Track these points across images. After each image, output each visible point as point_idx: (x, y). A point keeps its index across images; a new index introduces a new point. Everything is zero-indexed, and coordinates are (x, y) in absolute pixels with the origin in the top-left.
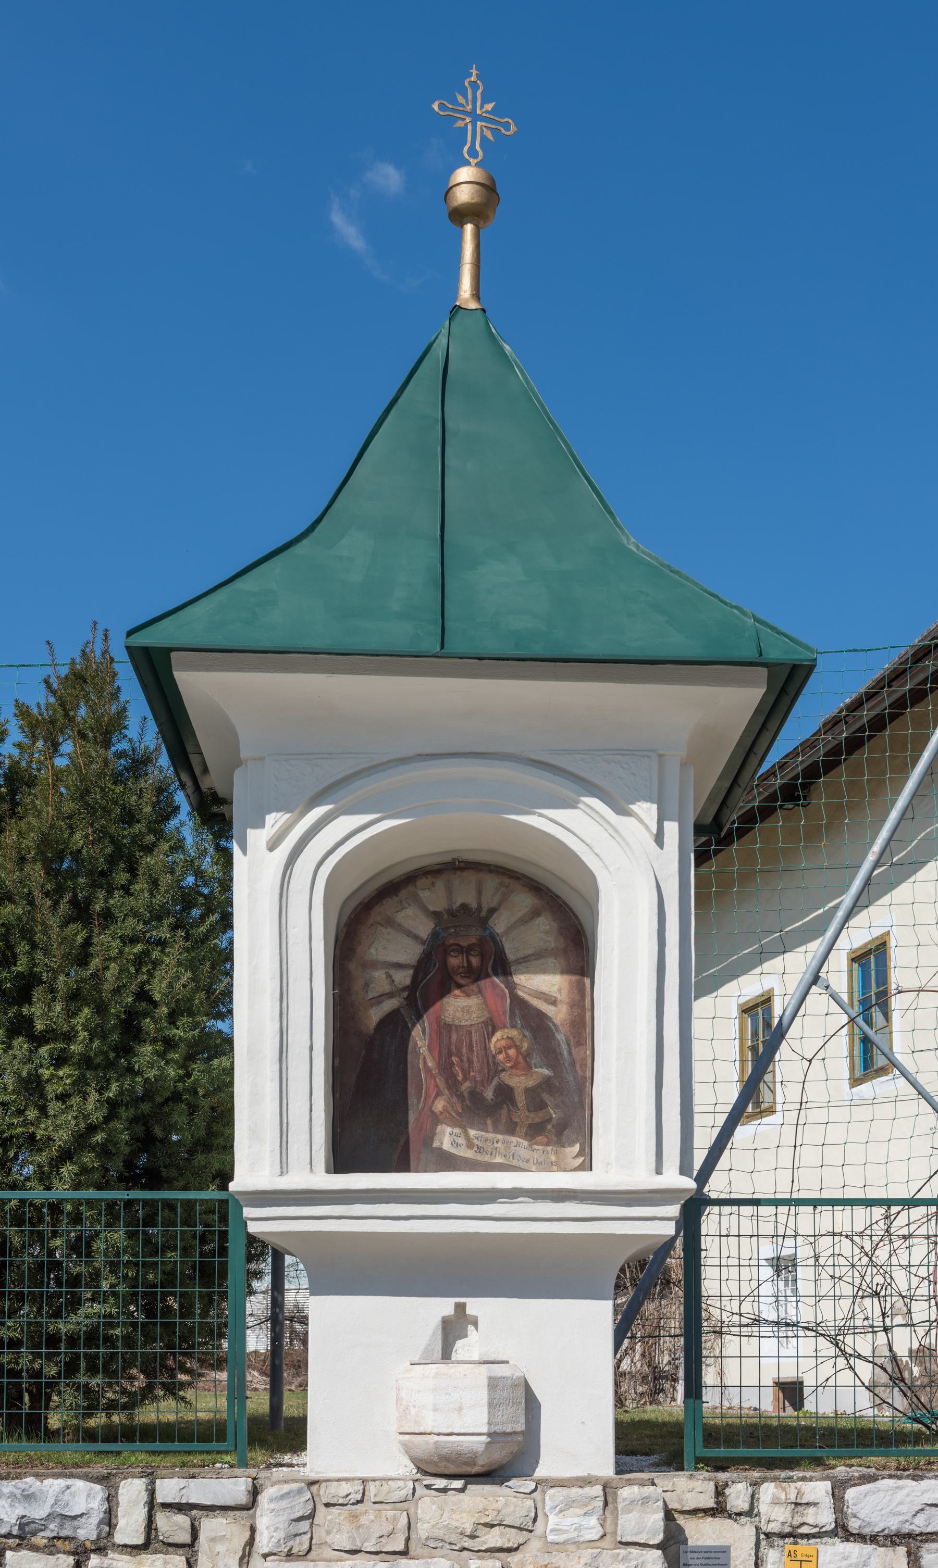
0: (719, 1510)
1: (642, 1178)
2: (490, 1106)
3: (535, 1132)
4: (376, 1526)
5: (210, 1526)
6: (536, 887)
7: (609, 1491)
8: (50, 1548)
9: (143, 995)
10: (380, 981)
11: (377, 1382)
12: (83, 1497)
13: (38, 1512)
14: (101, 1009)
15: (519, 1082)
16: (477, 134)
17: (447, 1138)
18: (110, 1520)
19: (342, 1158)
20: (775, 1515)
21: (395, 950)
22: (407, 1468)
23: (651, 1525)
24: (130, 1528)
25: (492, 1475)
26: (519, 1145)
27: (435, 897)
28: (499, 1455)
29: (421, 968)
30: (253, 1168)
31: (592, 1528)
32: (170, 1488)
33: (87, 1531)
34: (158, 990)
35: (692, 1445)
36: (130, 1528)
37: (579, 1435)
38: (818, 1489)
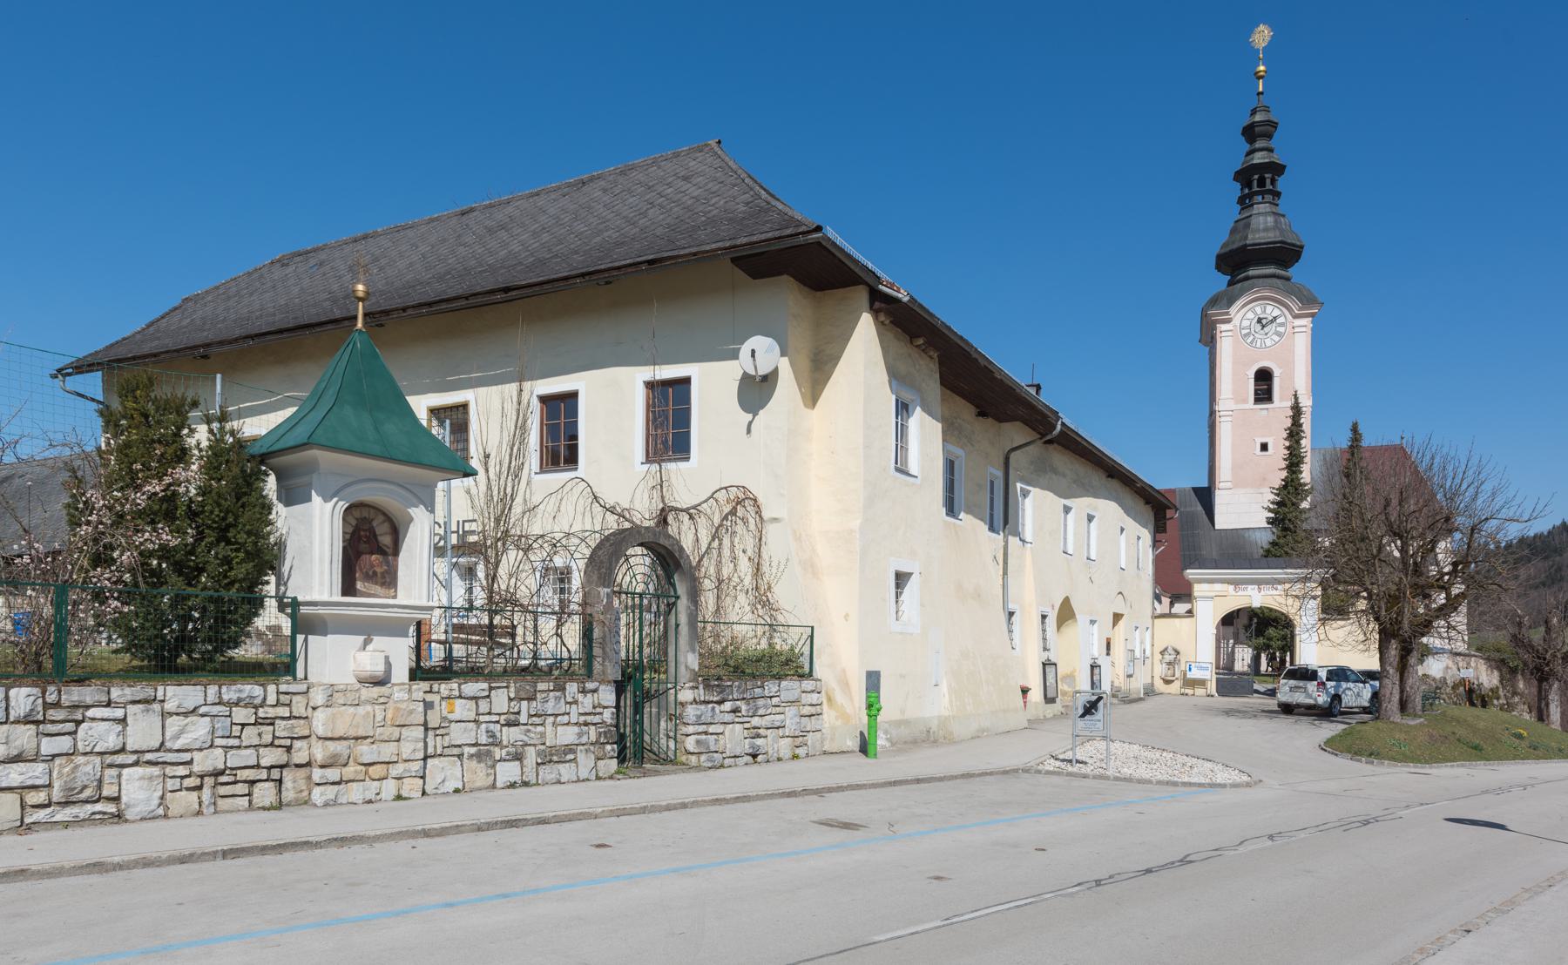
2: (371, 577)
3: (383, 585)
8: (246, 706)
11: (333, 661)
12: (258, 691)
13: (244, 695)
15: (379, 570)
17: (359, 585)
18: (265, 699)
20: (445, 693)
22: (354, 681)
24: (272, 699)
26: (378, 589)
32: (283, 688)
36: (272, 699)
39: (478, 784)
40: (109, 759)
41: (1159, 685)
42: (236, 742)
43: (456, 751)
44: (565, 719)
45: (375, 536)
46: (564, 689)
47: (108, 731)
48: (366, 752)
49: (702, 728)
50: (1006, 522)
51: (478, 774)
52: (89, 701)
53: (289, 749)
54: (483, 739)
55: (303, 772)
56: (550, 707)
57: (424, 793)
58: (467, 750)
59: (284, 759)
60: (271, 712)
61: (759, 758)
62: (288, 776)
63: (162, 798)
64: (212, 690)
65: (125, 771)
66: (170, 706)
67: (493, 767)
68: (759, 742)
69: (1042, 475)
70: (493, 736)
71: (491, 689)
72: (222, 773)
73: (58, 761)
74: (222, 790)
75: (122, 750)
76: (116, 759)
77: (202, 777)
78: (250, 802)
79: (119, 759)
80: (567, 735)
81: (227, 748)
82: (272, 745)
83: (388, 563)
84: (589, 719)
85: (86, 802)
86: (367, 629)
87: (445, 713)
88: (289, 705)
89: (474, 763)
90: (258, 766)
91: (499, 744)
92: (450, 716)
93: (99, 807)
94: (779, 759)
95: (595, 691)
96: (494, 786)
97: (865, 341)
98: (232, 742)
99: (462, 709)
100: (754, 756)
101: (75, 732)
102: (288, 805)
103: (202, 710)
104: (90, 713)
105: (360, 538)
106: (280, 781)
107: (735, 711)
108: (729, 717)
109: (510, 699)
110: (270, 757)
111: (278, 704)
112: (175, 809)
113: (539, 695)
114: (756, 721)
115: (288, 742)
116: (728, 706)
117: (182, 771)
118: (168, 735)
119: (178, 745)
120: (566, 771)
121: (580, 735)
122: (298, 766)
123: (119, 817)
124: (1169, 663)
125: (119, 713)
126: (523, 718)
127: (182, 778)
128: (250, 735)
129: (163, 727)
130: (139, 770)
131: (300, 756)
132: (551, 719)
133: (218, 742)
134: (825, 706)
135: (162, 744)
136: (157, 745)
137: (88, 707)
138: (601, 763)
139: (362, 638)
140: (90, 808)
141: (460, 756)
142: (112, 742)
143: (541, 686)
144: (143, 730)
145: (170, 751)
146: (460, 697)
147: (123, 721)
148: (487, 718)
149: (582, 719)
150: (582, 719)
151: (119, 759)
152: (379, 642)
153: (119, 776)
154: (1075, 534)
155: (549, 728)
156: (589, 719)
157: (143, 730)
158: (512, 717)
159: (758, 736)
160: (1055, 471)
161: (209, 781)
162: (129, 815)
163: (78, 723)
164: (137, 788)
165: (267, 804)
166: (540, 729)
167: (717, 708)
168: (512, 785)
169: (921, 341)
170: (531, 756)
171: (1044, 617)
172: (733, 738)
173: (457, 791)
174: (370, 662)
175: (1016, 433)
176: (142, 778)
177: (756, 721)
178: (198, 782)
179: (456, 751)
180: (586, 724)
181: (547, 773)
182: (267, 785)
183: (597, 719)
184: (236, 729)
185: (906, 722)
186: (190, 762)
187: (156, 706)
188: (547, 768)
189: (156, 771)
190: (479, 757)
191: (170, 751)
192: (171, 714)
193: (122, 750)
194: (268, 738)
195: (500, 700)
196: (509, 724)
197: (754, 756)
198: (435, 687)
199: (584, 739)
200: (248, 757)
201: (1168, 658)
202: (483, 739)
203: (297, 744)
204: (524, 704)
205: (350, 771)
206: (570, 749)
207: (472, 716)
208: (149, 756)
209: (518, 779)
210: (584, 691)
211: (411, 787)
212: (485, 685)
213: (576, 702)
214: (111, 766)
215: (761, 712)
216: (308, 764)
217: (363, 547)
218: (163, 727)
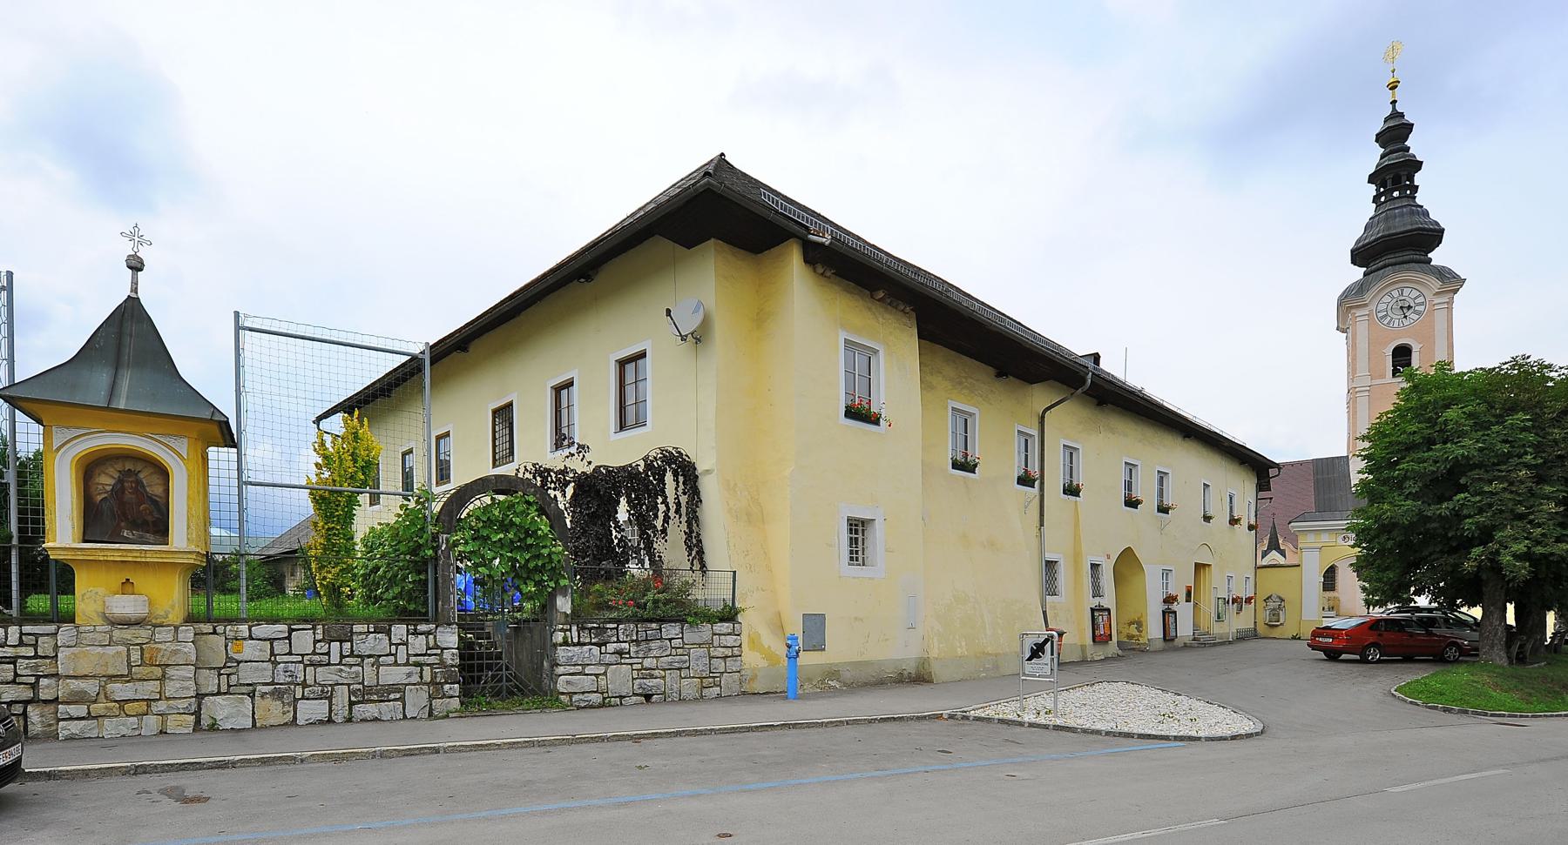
0: (215, 632)
3: (155, 533)
7: (176, 628)
20: (231, 634)
21: (106, 481)
26: (151, 537)
27: (119, 466)
39: (272, 722)
43: (245, 689)
48: (120, 690)
51: (274, 711)
55: (51, 708)
59: (29, 694)
68: (650, 683)
71: (291, 631)
80: (392, 675)
82: (14, 682)
86: (127, 577)
88: (35, 646)
89: (268, 700)
92: (236, 656)
99: (249, 650)
100: (648, 697)
107: (620, 653)
108: (614, 658)
109: (316, 642)
111: (21, 644)
114: (648, 663)
115: (32, 680)
116: (611, 647)
120: (388, 709)
122: (46, 702)
138: (436, 703)
141: (252, 695)
146: (251, 638)
148: (286, 658)
149: (412, 659)
159: (652, 677)
167: (596, 650)
180: (416, 664)
183: (432, 660)
197: (648, 697)
198: (220, 629)
201: (1272, 605)
202: (281, 678)
203: (44, 682)
205: (97, 708)
206: (395, 688)
210: (416, 633)
213: (406, 644)
215: (654, 653)
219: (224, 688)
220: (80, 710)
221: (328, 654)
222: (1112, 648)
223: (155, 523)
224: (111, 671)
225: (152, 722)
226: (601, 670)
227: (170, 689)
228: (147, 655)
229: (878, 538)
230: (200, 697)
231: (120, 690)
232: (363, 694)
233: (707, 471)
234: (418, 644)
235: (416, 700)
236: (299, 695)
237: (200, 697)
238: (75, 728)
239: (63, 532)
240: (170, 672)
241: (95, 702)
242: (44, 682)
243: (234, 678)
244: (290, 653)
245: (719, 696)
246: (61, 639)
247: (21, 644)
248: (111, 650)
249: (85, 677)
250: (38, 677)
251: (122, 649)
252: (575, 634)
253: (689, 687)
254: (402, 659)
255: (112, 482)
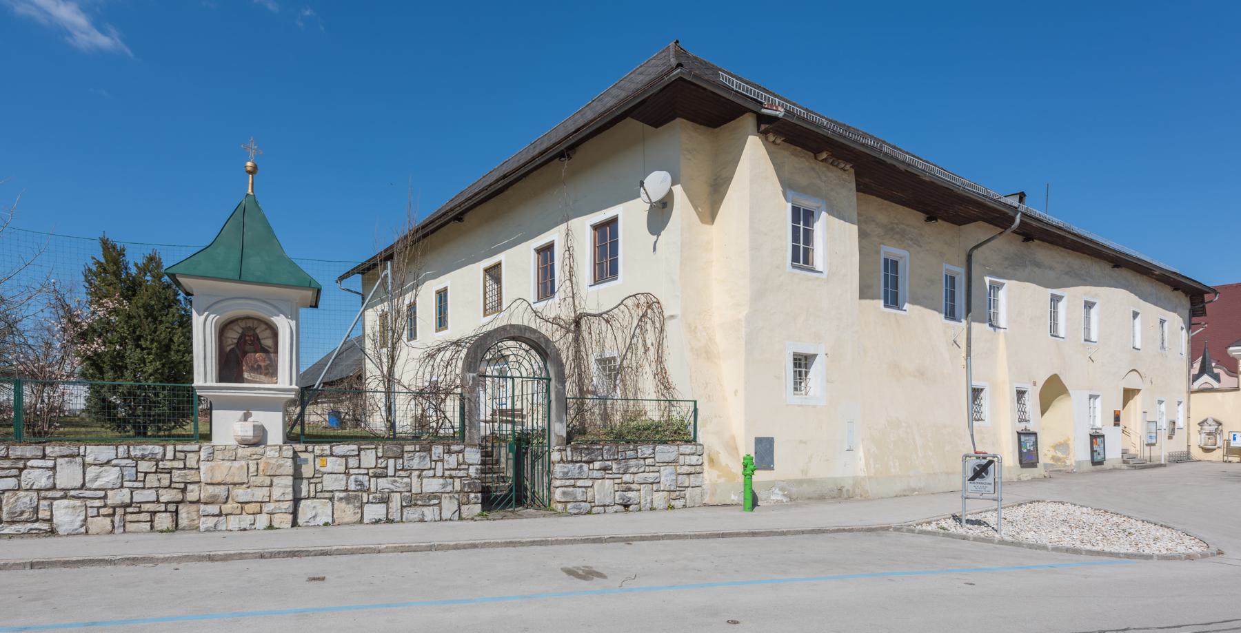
0: (306, 451)
1: (287, 386)
2: (256, 369)
3: (266, 374)
4: (227, 454)
5: (189, 455)
6: (266, 323)
8: (150, 460)
9: (171, 340)
10: (230, 341)
12: (158, 449)
14: (160, 343)
15: (262, 364)
16: (252, 153)
17: (246, 375)
18: (164, 455)
19: (221, 379)
20: (318, 452)
21: (233, 335)
23: (290, 453)
24: (170, 455)
25: (256, 445)
27: (243, 324)
28: (256, 440)
29: (239, 339)
30: (198, 381)
31: (277, 454)
32: (179, 447)
33: (159, 457)
34: (175, 339)
35: (303, 438)
36: (170, 455)
37: (276, 435)
38: (327, 447)
39: (346, 520)
40: (43, 494)
41: (1196, 453)
42: (141, 485)
43: (327, 495)
44: (431, 473)
45: (258, 339)
46: (430, 450)
47: (41, 476)
48: (241, 494)
49: (568, 482)
50: (969, 310)
51: (347, 512)
52: (28, 455)
53: (184, 490)
54: (352, 486)
55: (194, 507)
56: (415, 463)
57: (295, 524)
58: (337, 494)
59: (180, 497)
60: (168, 465)
61: (631, 508)
62: (183, 509)
63: (85, 520)
64: (122, 449)
65: (55, 503)
66: (89, 459)
67: (362, 507)
68: (630, 494)
69: (1016, 269)
70: (361, 484)
71: (360, 450)
72: (130, 505)
73: (6, 494)
74: (129, 517)
75: (54, 488)
76: (51, 492)
77: (114, 508)
78: (152, 527)
79: (50, 494)
81: (132, 490)
82: (169, 487)
83: (270, 359)
84: (453, 473)
85: (26, 521)
86: (247, 407)
87: (318, 467)
89: (343, 505)
90: (158, 501)
91: (368, 491)
92: (322, 469)
93: (36, 525)
94: (652, 509)
95: (460, 452)
96: (361, 521)
97: (754, 157)
98: (136, 484)
99: (333, 464)
100: (626, 506)
101: (20, 475)
102: (183, 529)
103: (114, 462)
104: (29, 463)
105: (245, 341)
106: (177, 512)
107: (605, 469)
109: (377, 458)
110: (166, 496)
111: (175, 458)
112: (92, 529)
113: (405, 455)
114: (627, 478)
115: (182, 486)
116: (597, 465)
117: (98, 503)
118: (87, 479)
119: (95, 485)
120: (429, 513)
121: (444, 486)
123: (53, 532)
124: (1210, 434)
125: (50, 463)
126: (391, 472)
127: (99, 508)
128: (152, 480)
129: (84, 473)
130: (65, 502)
131: (191, 496)
132: (417, 473)
133: (126, 484)
134: (706, 466)
135: (83, 486)
136: (79, 485)
137: (29, 459)
138: (464, 508)
139: (241, 413)
140: (29, 526)
141: (331, 499)
142: (43, 481)
143: (407, 448)
144: (68, 475)
145: (90, 489)
146: (332, 455)
147: (54, 468)
148: (356, 471)
149: (447, 473)
150: (447, 473)
151: (50, 494)
152: (258, 417)
153: (51, 505)
154: (1068, 320)
155: (415, 480)
156: (453, 473)
157: (68, 475)
158: (379, 471)
159: (630, 490)
160: (1038, 265)
161: (119, 511)
162: (61, 531)
163: (21, 470)
164: (65, 515)
165: (165, 528)
166: (406, 480)
167: (585, 467)
168: (378, 522)
169: (824, 155)
170: (396, 501)
171: (1021, 394)
172: (604, 490)
173: (326, 524)
174: (246, 430)
175: (977, 232)
176: (67, 507)
177: (627, 478)
178: (111, 511)
179: (327, 495)
180: (451, 477)
181: (411, 513)
182: (164, 515)
183: (462, 473)
184: (141, 476)
185: (810, 482)
186: (105, 497)
187: (78, 460)
188: (411, 510)
189: (78, 503)
190: (348, 500)
191: (90, 489)
192: (90, 465)
193: (54, 488)
194: (166, 482)
195: (369, 458)
196: (377, 476)
197: (626, 506)
198: (310, 448)
199: (449, 488)
200: (150, 495)
203: (190, 487)
204: (391, 461)
207: (342, 469)
208: (72, 493)
209: (383, 517)
210: (449, 452)
211: (283, 520)
212: (355, 447)
213: (442, 460)
214: (45, 498)
215: (632, 470)
216: (198, 502)
217: (248, 348)
218: (84, 473)
219: (312, 495)
220: (214, 509)
221: (386, 468)
222: (1038, 471)
223: (267, 367)
224: (236, 480)
225: (263, 520)
226: (589, 483)
227: (277, 493)
228: (261, 468)
229: (816, 372)
230: (297, 500)
231: (241, 494)
232: (412, 501)
233: (672, 317)
234: (452, 461)
235: (449, 507)
236: (365, 500)
237: (297, 500)
238: (211, 522)
239: (204, 374)
240: (276, 480)
241: (226, 502)
242: (190, 487)
243: (319, 486)
244: (359, 467)
245: (685, 506)
246: (203, 455)
247: (175, 458)
248: (236, 464)
249: (219, 484)
250: (186, 483)
251: (243, 463)
252: (569, 453)
253: (659, 499)
254: (439, 473)
255: (237, 336)
